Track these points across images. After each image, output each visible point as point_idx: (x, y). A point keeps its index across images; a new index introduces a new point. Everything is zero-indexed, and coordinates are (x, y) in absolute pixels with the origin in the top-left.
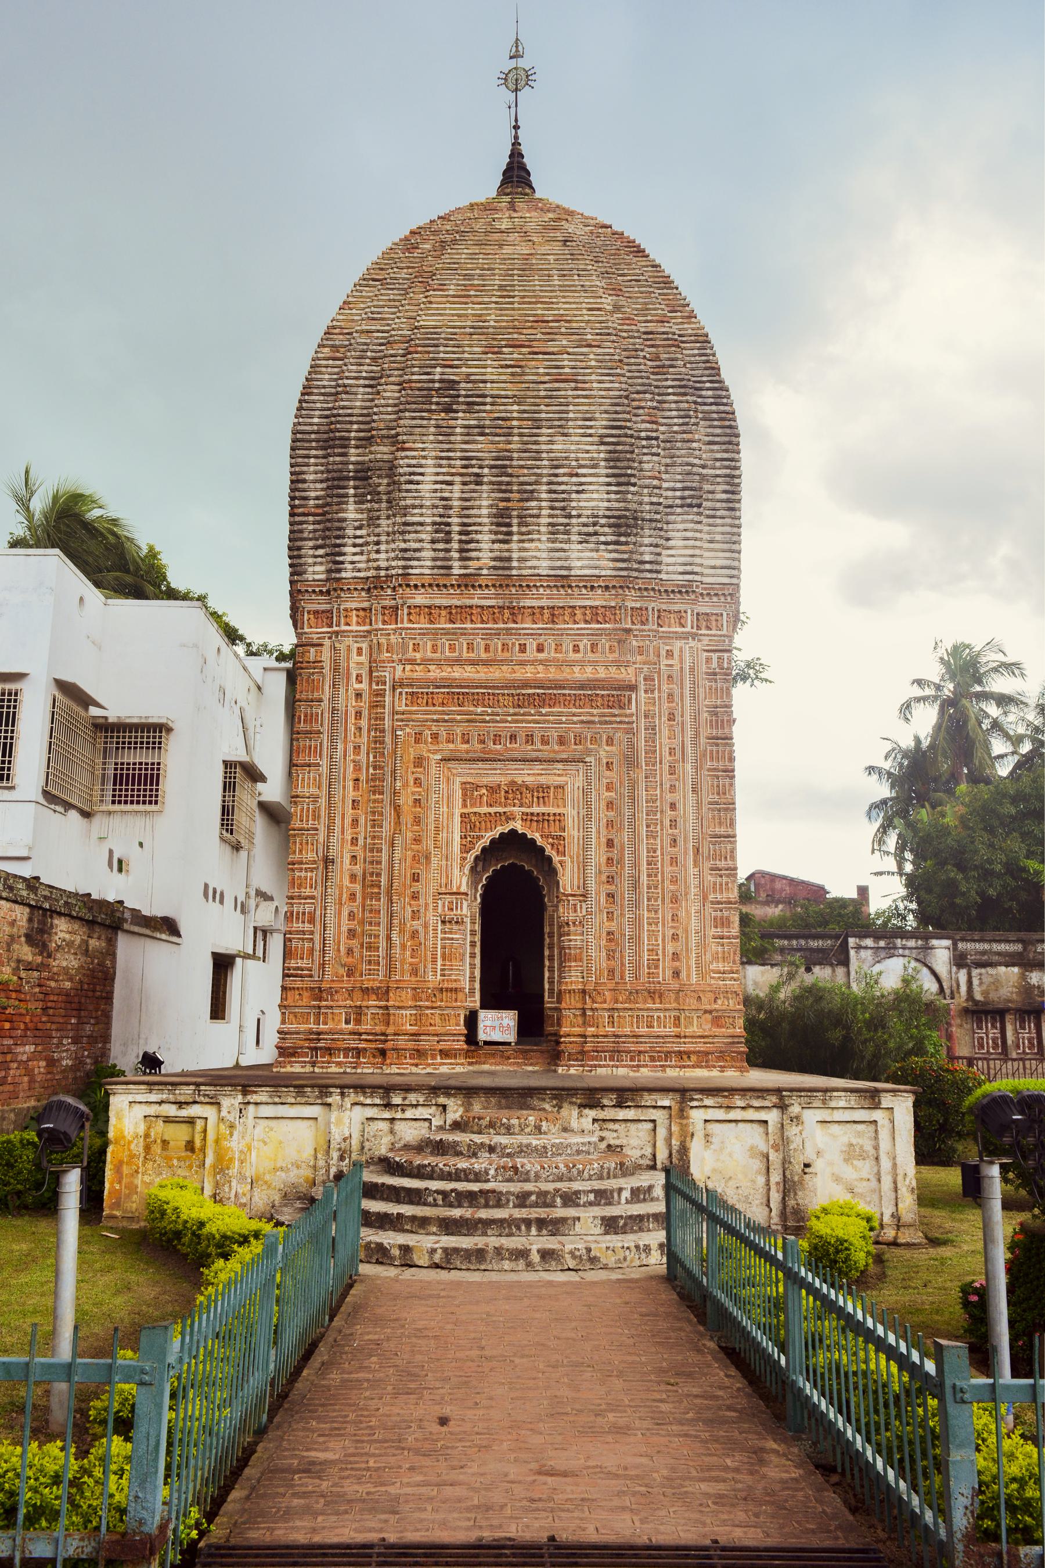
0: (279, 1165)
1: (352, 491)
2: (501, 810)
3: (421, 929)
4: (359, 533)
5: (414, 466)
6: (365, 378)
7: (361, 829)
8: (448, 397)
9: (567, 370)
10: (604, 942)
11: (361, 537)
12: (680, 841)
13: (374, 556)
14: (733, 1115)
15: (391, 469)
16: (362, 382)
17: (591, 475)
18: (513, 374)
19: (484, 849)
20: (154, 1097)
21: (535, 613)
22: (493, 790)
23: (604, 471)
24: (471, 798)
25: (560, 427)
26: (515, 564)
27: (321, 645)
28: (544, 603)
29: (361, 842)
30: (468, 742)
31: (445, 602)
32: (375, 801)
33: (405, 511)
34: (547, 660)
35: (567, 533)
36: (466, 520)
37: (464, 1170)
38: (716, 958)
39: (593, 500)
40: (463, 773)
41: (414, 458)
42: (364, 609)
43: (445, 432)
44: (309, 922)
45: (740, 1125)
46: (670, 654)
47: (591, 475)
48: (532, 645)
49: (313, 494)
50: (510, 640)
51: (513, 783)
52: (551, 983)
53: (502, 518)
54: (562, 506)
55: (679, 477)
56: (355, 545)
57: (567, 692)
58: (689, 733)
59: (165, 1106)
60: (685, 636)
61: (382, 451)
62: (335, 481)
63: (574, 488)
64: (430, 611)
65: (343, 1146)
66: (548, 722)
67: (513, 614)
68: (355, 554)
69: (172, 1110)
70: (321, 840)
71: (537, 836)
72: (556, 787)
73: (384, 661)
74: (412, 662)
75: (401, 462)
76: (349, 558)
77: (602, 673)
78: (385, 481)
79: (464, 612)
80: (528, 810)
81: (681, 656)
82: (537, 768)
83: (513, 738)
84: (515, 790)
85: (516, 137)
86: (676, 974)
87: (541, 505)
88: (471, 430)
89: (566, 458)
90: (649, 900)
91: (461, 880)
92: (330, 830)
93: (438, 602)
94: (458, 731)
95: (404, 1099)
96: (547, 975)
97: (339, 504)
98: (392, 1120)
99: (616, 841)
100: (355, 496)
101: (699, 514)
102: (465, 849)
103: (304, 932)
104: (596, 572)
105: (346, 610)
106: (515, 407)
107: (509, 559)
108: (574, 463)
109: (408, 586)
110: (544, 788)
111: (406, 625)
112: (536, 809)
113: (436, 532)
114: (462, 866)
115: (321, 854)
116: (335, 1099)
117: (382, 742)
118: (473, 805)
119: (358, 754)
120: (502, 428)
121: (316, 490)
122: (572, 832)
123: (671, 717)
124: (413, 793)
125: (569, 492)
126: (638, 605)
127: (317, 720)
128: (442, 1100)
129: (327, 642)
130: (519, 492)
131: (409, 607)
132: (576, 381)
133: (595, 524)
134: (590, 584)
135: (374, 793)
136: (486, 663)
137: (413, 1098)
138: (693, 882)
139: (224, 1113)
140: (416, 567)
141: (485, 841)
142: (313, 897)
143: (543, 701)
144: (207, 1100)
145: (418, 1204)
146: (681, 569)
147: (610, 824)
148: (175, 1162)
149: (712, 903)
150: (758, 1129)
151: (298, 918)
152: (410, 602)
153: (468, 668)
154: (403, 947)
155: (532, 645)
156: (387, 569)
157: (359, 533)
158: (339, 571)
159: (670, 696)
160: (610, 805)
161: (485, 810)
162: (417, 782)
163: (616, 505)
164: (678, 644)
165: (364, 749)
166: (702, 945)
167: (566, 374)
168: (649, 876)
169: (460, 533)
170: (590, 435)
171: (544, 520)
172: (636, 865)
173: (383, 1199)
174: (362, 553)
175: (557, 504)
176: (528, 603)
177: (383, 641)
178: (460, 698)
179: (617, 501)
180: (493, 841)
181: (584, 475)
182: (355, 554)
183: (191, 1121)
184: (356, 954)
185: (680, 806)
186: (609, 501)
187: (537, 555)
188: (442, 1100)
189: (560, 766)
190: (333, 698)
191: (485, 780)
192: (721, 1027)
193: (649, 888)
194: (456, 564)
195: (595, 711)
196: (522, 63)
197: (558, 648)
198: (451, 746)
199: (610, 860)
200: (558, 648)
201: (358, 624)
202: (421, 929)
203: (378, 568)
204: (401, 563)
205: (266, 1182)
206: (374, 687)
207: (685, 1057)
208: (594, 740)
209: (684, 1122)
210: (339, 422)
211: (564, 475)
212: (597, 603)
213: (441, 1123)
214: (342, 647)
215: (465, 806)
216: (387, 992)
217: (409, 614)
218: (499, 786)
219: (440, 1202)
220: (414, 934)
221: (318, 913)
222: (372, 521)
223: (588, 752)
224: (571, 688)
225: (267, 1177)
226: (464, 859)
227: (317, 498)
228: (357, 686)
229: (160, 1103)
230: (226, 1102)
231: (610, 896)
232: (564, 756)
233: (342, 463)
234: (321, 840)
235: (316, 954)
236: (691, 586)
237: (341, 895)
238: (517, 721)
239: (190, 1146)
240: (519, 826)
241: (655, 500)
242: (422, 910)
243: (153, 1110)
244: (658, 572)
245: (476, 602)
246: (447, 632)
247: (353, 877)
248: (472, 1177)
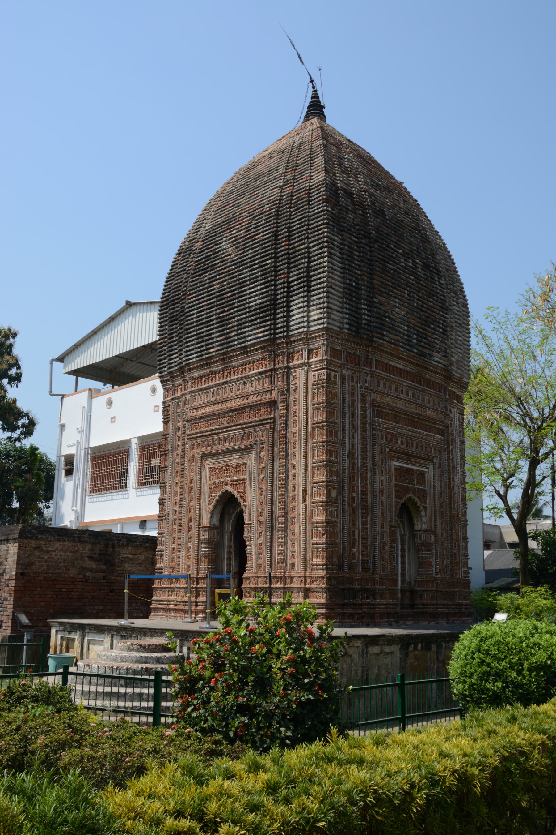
2: (223, 480)
40: (209, 463)
51: (227, 466)
60: (301, 366)
71: (235, 493)
80: (233, 479)
82: (237, 456)
112: (236, 478)
141: (217, 498)
191: (216, 466)
215: (210, 480)
238: (227, 431)
240: (228, 488)
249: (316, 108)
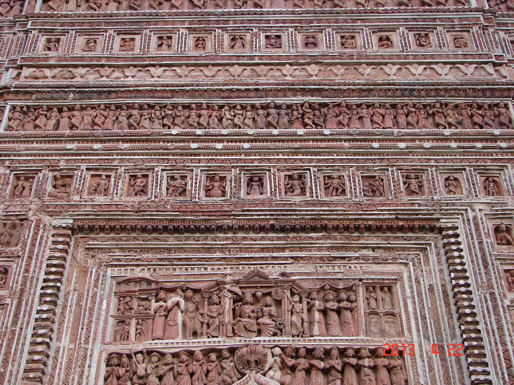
2: (223, 342)
22: (202, 296)
30: (143, 191)
72: (371, 287)
80: (301, 343)
112: (320, 340)
161: (178, 342)
189: (373, 240)
191: (179, 274)
218: (219, 285)
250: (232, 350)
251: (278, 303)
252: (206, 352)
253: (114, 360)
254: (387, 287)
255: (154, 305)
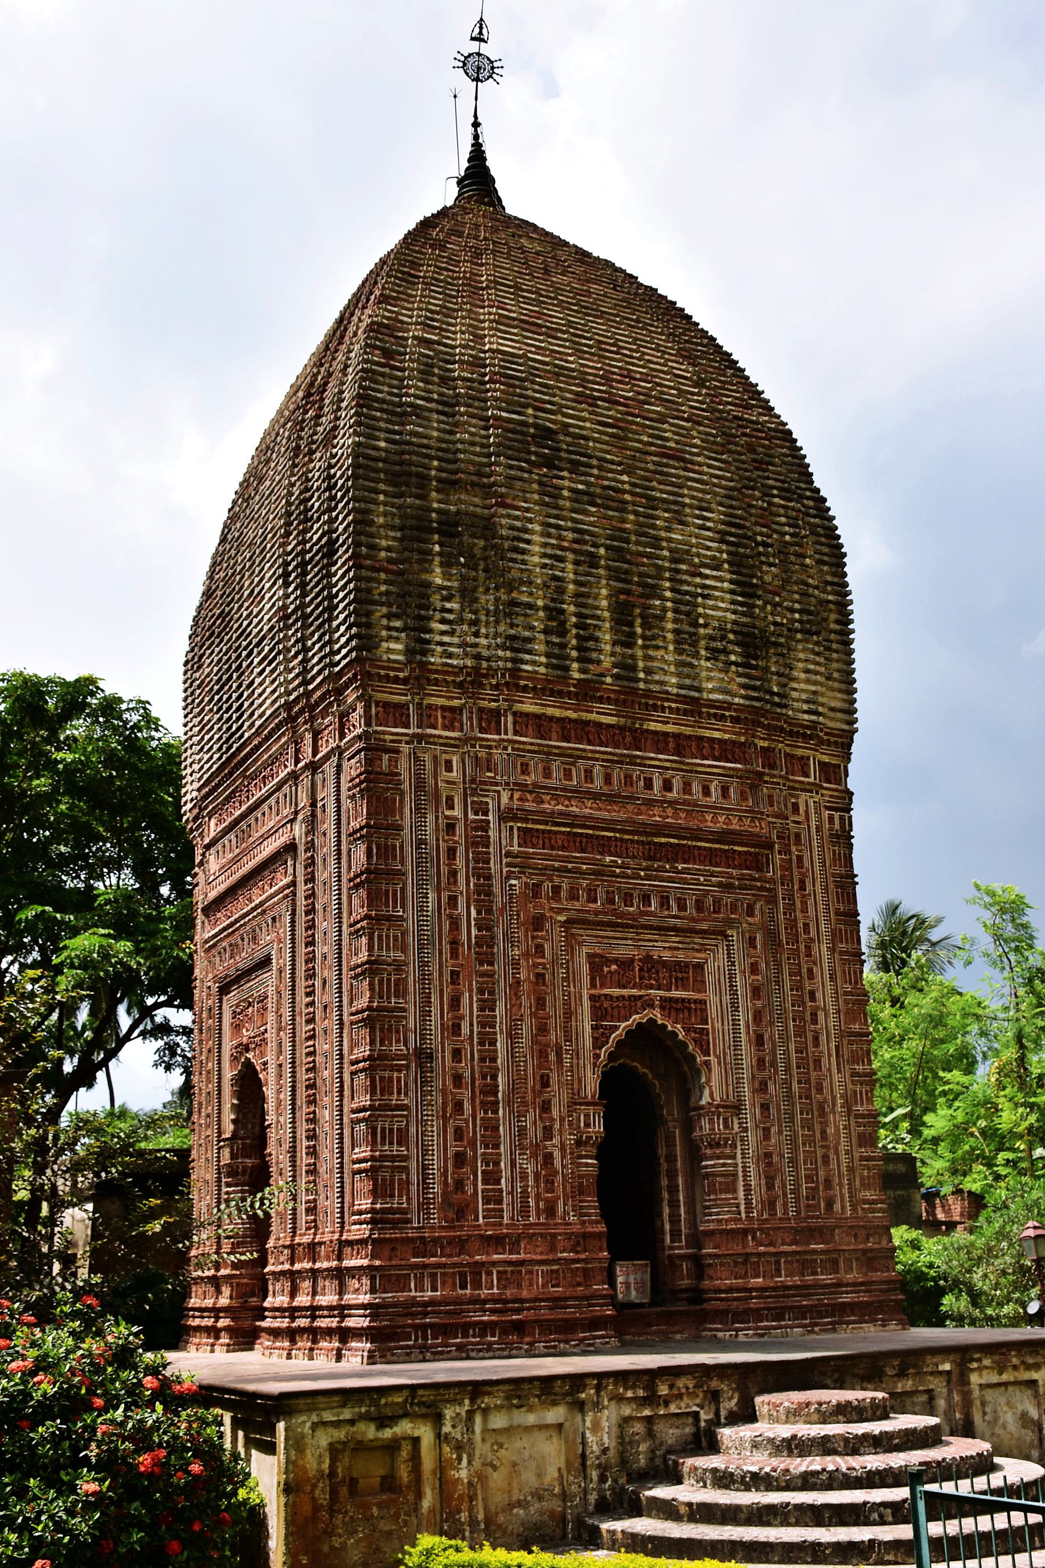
0: (515, 1498)
1: (437, 548)
2: (635, 992)
3: (557, 1154)
4: (448, 605)
5: (518, 529)
6: (437, 402)
7: (465, 1010)
8: (542, 447)
9: (672, 444)
10: (762, 1166)
11: (450, 611)
12: (823, 1038)
13: (471, 639)
14: (1005, 1377)
15: (487, 528)
16: (433, 405)
17: (715, 578)
18: (612, 435)
19: (620, 1043)
20: (347, 1414)
21: (661, 741)
22: (626, 964)
23: (728, 576)
24: (603, 977)
25: (676, 512)
26: (642, 675)
27: (397, 751)
28: (670, 728)
29: (465, 1029)
30: (595, 901)
31: (557, 713)
32: (483, 974)
33: (511, 586)
34: (676, 802)
35: (694, 644)
36: (583, 611)
37: (878, 1472)
38: (865, 1186)
39: (718, 608)
41: (517, 518)
42: (452, 709)
43: (550, 492)
44: (399, 1144)
45: (1010, 1388)
46: (796, 808)
47: (715, 578)
48: (657, 784)
49: (384, 543)
50: (636, 771)
51: (648, 958)
52: (675, 1219)
53: (622, 614)
54: (687, 610)
55: (797, 596)
56: (443, 621)
57: (703, 844)
58: (821, 907)
59: (361, 1426)
61: (468, 502)
62: (415, 530)
63: (699, 591)
64: (540, 724)
65: (603, 1459)
66: (685, 881)
67: (635, 738)
68: (443, 633)
69: (370, 1432)
70: (411, 1025)
73: (485, 783)
74: (522, 787)
75: (504, 521)
76: (438, 638)
77: (735, 826)
78: (482, 543)
79: (583, 730)
80: (668, 994)
81: (807, 812)
83: (646, 899)
84: (651, 965)
85: (476, 137)
86: (830, 1205)
87: (665, 601)
88: (580, 497)
89: (688, 552)
90: (802, 1113)
91: (591, 1084)
92: (425, 1014)
93: (550, 711)
94: (585, 883)
95: (671, 1387)
96: (666, 1211)
97: (420, 562)
98: (649, 1420)
99: (766, 1037)
100: (440, 554)
101: (817, 643)
102: (598, 1044)
103: (393, 1158)
104: (729, 698)
105: (430, 706)
106: (625, 478)
107: (634, 668)
108: (696, 560)
109: (517, 686)
110: (680, 967)
111: (510, 736)
112: (676, 994)
113: (549, 619)
114: (595, 1065)
115: (412, 1045)
116: (587, 1394)
117: (489, 894)
118: (602, 986)
119: (455, 907)
120: (611, 500)
121: (387, 537)
122: (716, 1024)
123: (802, 887)
124: (535, 965)
125: (695, 595)
126: (766, 744)
127: (394, 858)
128: (714, 1384)
129: (405, 748)
130: (638, 584)
131: (515, 714)
132: (684, 460)
133: (723, 638)
134: (719, 711)
135: (481, 964)
136: (611, 798)
137: (681, 1383)
138: (838, 1091)
139: (447, 1429)
140: (527, 663)
142: (406, 1108)
143: (676, 854)
144: (424, 1410)
145: (856, 1524)
146: (805, 707)
147: (758, 1015)
148: (375, 1511)
149: (857, 1116)
150: (1029, 1392)
151: (383, 1138)
152: (518, 707)
153: (589, 804)
154: (537, 1175)
155: (657, 784)
156: (488, 659)
157: (448, 605)
158: (424, 653)
159: (800, 859)
160: (756, 992)
161: (616, 992)
162: (540, 950)
163: (744, 620)
164: (803, 796)
165: (462, 902)
166: (851, 1170)
167: (670, 448)
168: (800, 1082)
169: (576, 626)
170: (708, 529)
171: (670, 626)
172: (788, 1069)
173: (797, 1524)
174: (452, 633)
175: (683, 608)
176: (653, 726)
177: (483, 754)
178: (584, 843)
179: (743, 614)
180: (629, 1033)
181: (707, 577)
182: (443, 633)
183: (392, 1447)
184: (469, 1190)
185: (819, 995)
186: (735, 612)
187: (664, 669)
188: (714, 1384)
190: (419, 826)
191: (615, 953)
192: (877, 1271)
193: (800, 1098)
194: (575, 665)
195: (735, 872)
196: (485, 49)
197: (687, 787)
198: (577, 905)
199: (761, 1061)
200: (687, 787)
201: (445, 728)
202: (557, 1154)
203: (478, 657)
204: (508, 654)
205: (500, 1526)
206: (471, 816)
207: (848, 1311)
208: (734, 908)
209: (966, 1389)
210: (410, 453)
211: (686, 572)
212: (727, 736)
213: (711, 1416)
214: (427, 758)
215: (593, 985)
216: (518, 1241)
217: (515, 723)
218: (632, 960)
219: (890, 1519)
220: (548, 1158)
221: (413, 1130)
222: (468, 595)
223: (729, 923)
224: (707, 841)
225: (501, 1519)
226: (597, 1056)
227: (388, 549)
228: (448, 813)
229: (352, 1422)
230: (449, 1413)
231: (765, 1107)
232: (704, 926)
233: (420, 508)
234: (411, 1025)
235: (414, 1189)
236: (815, 729)
237: (445, 1104)
239: (389, 1483)
241: (778, 619)
242: (557, 1126)
243: (340, 1434)
244: (785, 706)
245: (593, 717)
246: (563, 753)
247: (458, 1079)
248: (890, 1481)
249: (478, 179)
250: (640, 997)
251: (657, 972)
252: (630, 997)
253: (592, 998)
254: (699, 967)
255: (606, 969)
